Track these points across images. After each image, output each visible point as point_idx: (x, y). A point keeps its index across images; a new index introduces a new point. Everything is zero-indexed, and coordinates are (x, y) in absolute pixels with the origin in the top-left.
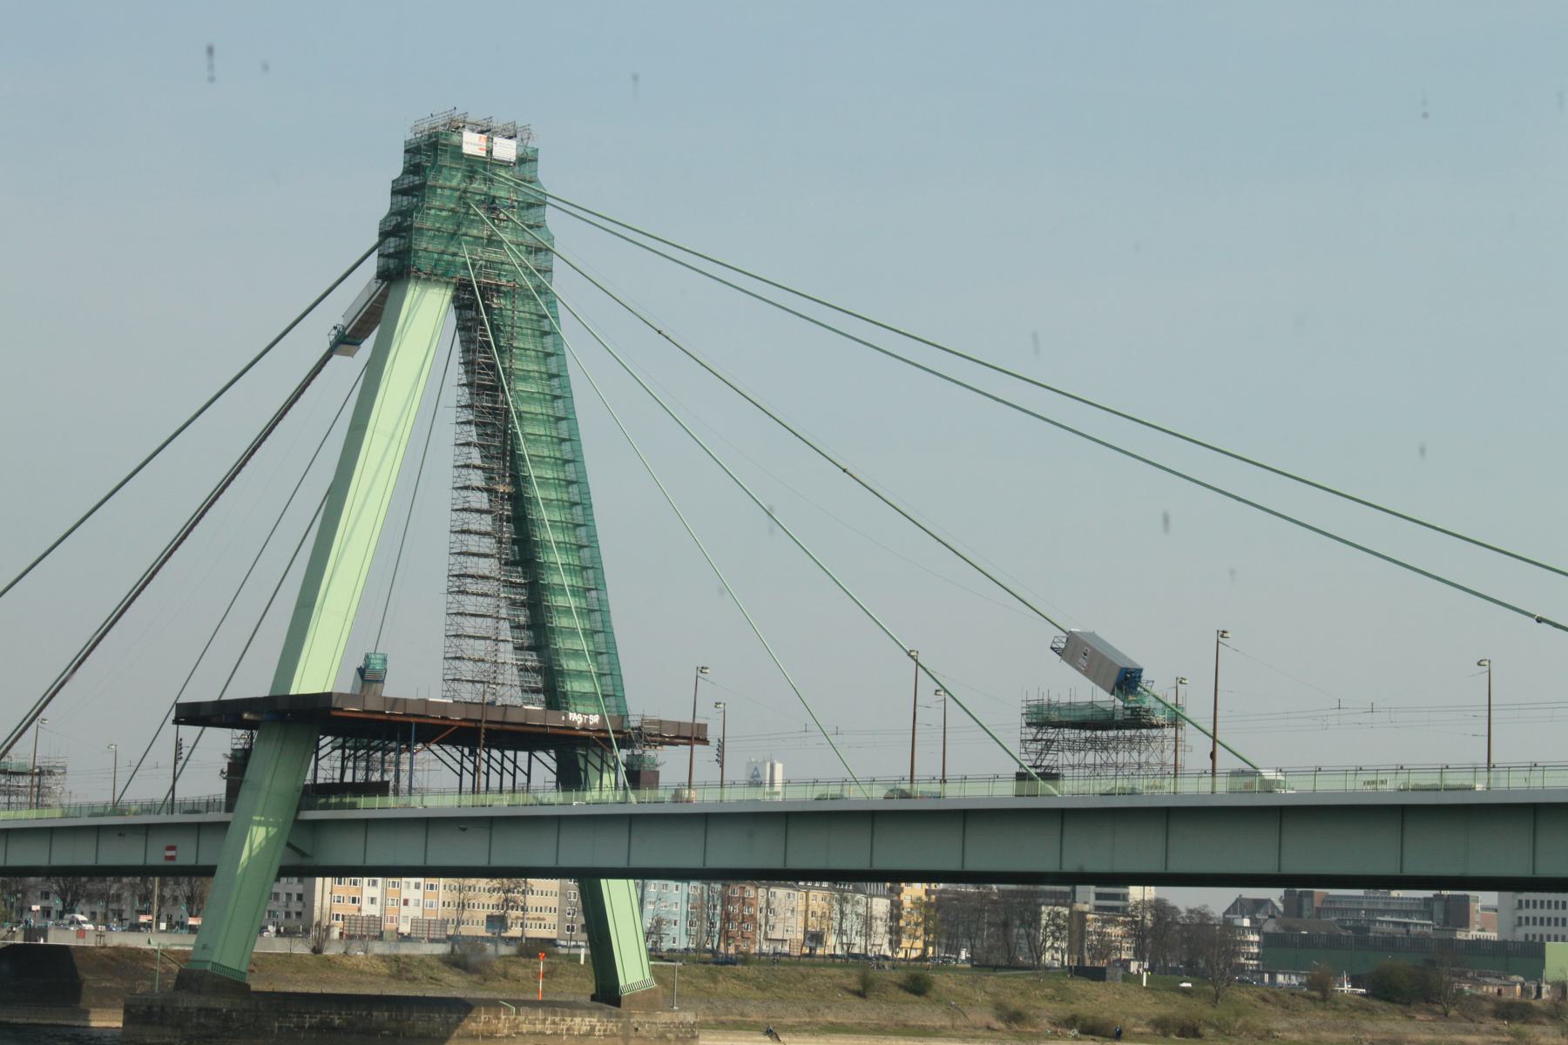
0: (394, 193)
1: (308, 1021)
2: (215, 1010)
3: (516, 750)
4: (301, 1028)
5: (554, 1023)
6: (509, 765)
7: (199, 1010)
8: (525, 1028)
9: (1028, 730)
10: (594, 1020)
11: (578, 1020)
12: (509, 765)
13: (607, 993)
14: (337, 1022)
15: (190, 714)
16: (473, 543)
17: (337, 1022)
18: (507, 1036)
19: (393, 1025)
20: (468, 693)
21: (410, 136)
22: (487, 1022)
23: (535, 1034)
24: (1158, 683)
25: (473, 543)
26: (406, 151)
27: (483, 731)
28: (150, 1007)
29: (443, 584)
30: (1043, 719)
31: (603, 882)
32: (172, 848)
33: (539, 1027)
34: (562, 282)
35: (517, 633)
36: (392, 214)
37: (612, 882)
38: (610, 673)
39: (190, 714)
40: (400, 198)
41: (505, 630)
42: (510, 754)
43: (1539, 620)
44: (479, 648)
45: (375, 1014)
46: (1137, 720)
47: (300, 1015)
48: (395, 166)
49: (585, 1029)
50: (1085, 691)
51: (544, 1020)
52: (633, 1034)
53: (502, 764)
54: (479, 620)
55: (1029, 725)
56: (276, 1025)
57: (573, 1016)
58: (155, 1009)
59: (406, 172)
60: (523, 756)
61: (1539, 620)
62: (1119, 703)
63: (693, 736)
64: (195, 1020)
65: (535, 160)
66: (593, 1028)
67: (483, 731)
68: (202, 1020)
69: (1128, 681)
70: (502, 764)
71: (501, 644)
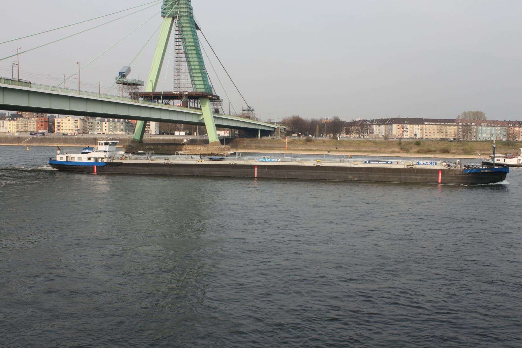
1: (147, 147)
4: (146, 149)
5: (193, 148)
8: (187, 149)
10: (201, 147)
11: (198, 147)
14: (152, 148)
17: (152, 148)
19: (162, 148)
22: (180, 148)
23: (189, 150)
33: (190, 148)
47: (145, 146)
49: (199, 149)
57: (197, 146)
66: (201, 149)
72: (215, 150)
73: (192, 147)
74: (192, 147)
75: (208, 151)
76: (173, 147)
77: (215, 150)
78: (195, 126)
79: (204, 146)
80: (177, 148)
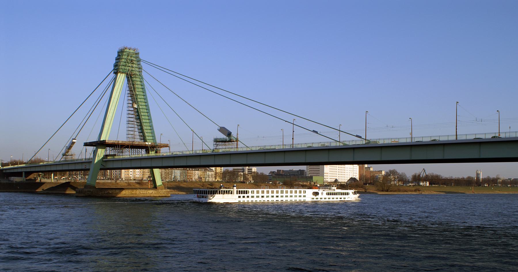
0: (116, 59)
2: (90, 191)
3: (139, 149)
4: (104, 193)
6: (138, 151)
7: (88, 191)
8: (141, 192)
9: (214, 143)
11: (150, 191)
12: (138, 151)
13: (155, 187)
15: (86, 144)
16: (131, 116)
17: (110, 192)
18: (139, 194)
20: (131, 140)
21: (118, 50)
22: (135, 192)
23: (143, 193)
24: (234, 134)
25: (131, 116)
26: (118, 53)
27: (130, 146)
28: (80, 191)
29: (126, 122)
30: (216, 141)
31: (154, 169)
32: (86, 166)
33: (144, 192)
34: (143, 74)
35: (139, 130)
36: (115, 63)
37: (155, 169)
38: (154, 136)
39: (86, 144)
40: (117, 60)
41: (137, 130)
42: (138, 149)
43: (286, 121)
44: (132, 133)
45: (117, 191)
46: (230, 141)
47: (104, 191)
48: (116, 55)
49: (151, 192)
50: (222, 136)
51: (144, 191)
52: (159, 193)
53: (137, 151)
54: (132, 128)
55: (214, 142)
56: (100, 193)
58: (81, 191)
59: (118, 56)
60: (140, 150)
61: (286, 121)
62: (228, 138)
63: (166, 146)
64: (87, 193)
65: (138, 54)
66: (153, 192)
67: (130, 146)
68: (88, 193)
69: (229, 134)
70: (137, 151)
71: (135, 132)
72: (164, 193)
73: (145, 191)
74: (145, 191)
75: (158, 194)
76: (130, 191)
77: (164, 193)
78: (110, 171)
79: (155, 190)
80: (133, 192)
